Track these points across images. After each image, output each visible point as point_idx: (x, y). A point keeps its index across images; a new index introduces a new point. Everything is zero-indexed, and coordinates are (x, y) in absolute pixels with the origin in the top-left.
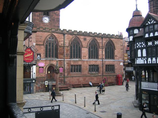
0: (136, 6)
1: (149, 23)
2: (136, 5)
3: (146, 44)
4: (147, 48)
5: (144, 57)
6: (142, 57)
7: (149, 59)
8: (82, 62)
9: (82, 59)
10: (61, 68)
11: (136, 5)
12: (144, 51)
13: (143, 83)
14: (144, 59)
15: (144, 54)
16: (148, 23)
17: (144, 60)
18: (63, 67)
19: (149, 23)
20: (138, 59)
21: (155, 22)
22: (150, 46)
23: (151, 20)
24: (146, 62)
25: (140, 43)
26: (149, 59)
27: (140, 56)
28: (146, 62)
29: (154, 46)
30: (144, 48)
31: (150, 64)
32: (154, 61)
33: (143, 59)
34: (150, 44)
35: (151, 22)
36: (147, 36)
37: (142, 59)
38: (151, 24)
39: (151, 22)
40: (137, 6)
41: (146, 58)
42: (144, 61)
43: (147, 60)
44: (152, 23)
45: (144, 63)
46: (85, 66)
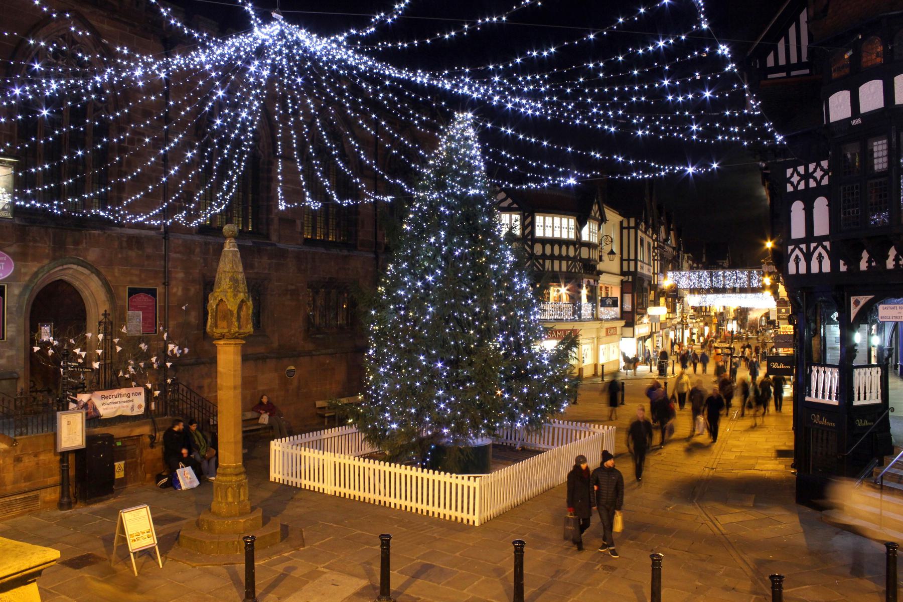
8: (274, 261)
9: (274, 238)
10: (142, 295)
18: (152, 292)
46: (290, 287)
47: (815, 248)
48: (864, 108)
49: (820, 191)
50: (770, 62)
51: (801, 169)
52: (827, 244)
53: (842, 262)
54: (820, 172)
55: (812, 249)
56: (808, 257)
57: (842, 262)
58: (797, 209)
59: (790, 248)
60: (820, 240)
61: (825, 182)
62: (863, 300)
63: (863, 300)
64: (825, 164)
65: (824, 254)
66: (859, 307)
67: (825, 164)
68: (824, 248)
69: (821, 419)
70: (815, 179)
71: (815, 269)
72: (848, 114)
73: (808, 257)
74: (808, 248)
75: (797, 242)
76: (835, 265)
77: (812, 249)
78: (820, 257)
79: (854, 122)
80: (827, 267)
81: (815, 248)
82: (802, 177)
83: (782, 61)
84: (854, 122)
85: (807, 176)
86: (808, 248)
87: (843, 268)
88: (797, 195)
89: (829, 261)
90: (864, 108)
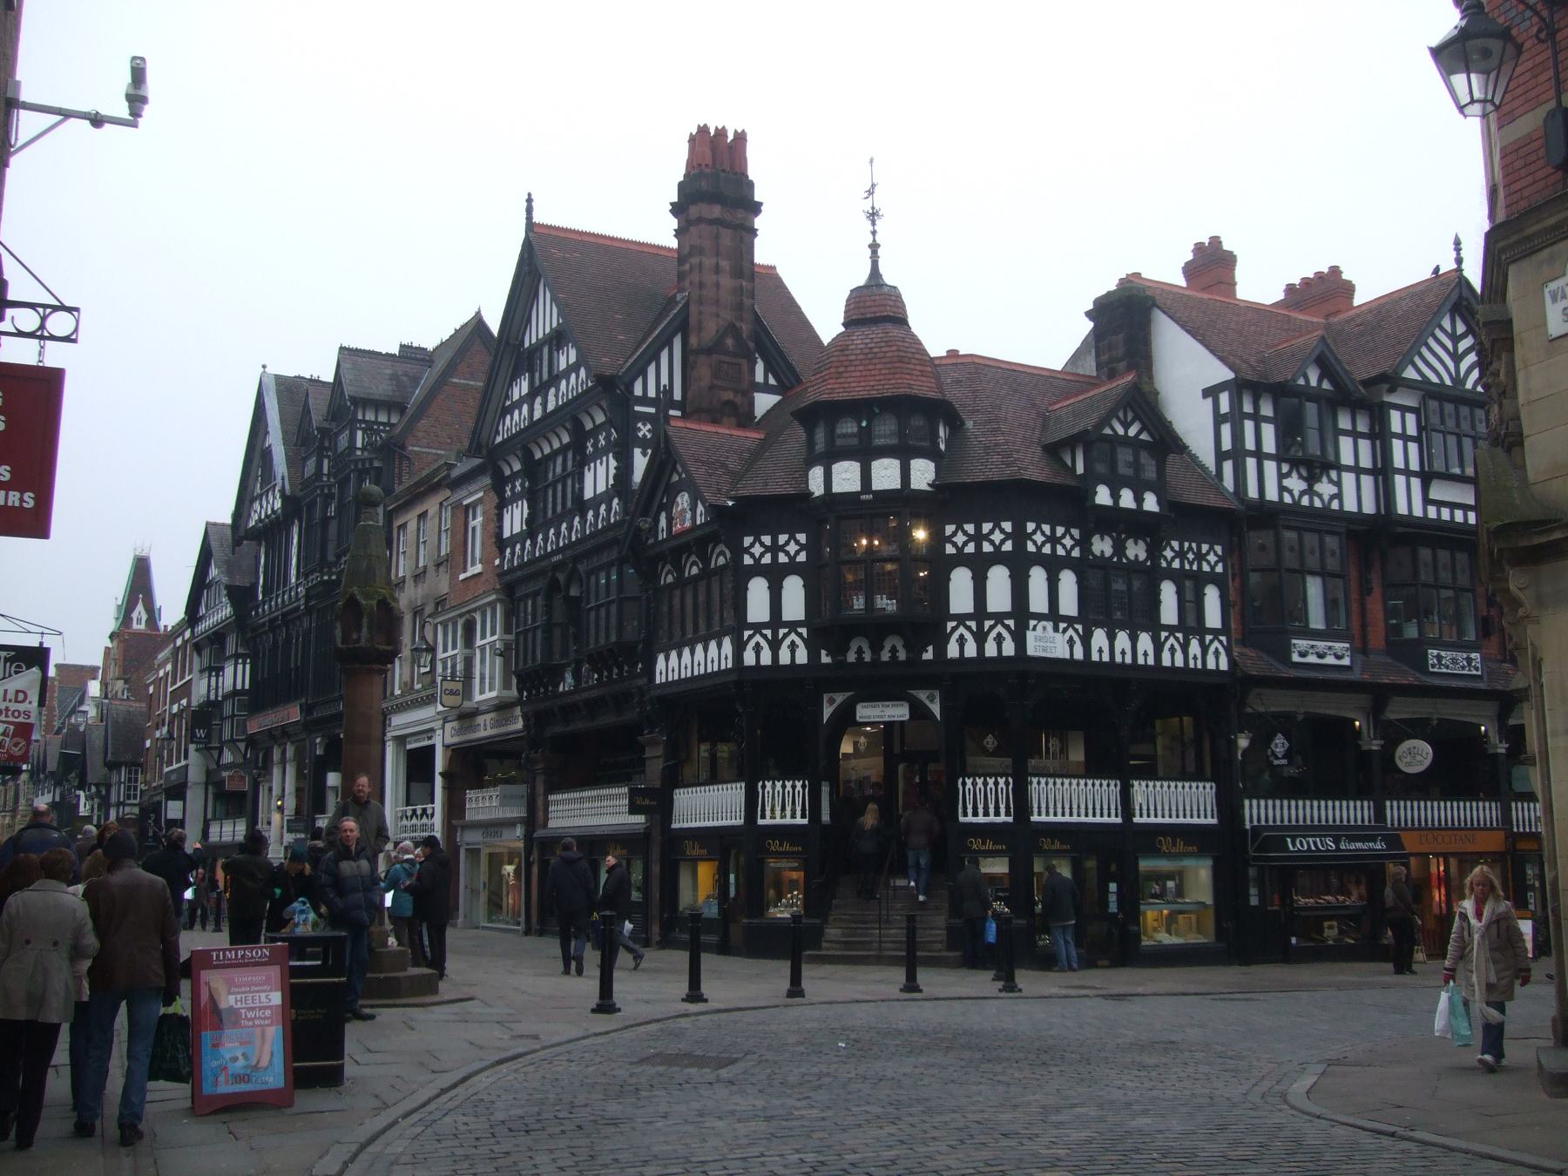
0: (869, 252)
1: (1121, 431)
2: (874, 247)
3: (1084, 543)
4: (1084, 567)
5: (1070, 621)
6: (1054, 615)
7: (1099, 638)
11: (874, 247)
12: (1068, 581)
13: (1035, 784)
14: (793, 636)
15: (1069, 603)
16: (1113, 429)
17: (1071, 637)
19: (1121, 431)
20: (1032, 623)
21: (1144, 436)
22: (1102, 563)
23: (1129, 420)
24: (1079, 654)
25: (1046, 528)
26: (1099, 638)
27: (1046, 611)
28: (1079, 654)
29: (1119, 567)
30: (998, 557)
31: (1146, 666)
32: (1123, 653)
33: (1065, 630)
34: (1102, 546)
35: (1126, 426)
36: (1103, 496)
37: (1056, 629)
38: (1126, 441)
39: (1126, 426)
40: (880, 252)
41: (1079, 627)
42: (1071, 642)
43: (1086, 640)
44: (1132, 432)
45: (1067, 656)
47: (786, 636)
48: (877, 485)
49: (792, 568)
50: (638, 391)
51: (767, 540)
52: (803, 631)
53: (823, 652)
54: (794, 546)
55: (780, 636)
56: (775, 645)
57: (823, 652)
58: (758, 591)
59: (747, 634)
60: (793, 626)
61: (802, 557)
62: (840, 698)
63: (840, 698)
64: (802, 537)
65: (798, 641)
66: (835, 705)
67: (802, 537)
68: (800, 635)
69: (781, 845)
70: (787, 553)
71: (785, 657)
72: (855, 486)
73: (775, 645)
74: (775, 634)
75: (758, 628)
76: (813, 655)
77: (780, 636)
78: (793, 646)
79: (863, 497)
80: (802, 657)
81: (786, 636)
82: (782, 549)
83: (652, 393)
84: (863, 497)
85: (775, 549)
86: (775, 634)
87: (825, 659)
88: (758, 570)
89: (806, 651)
90: (877, 485)
